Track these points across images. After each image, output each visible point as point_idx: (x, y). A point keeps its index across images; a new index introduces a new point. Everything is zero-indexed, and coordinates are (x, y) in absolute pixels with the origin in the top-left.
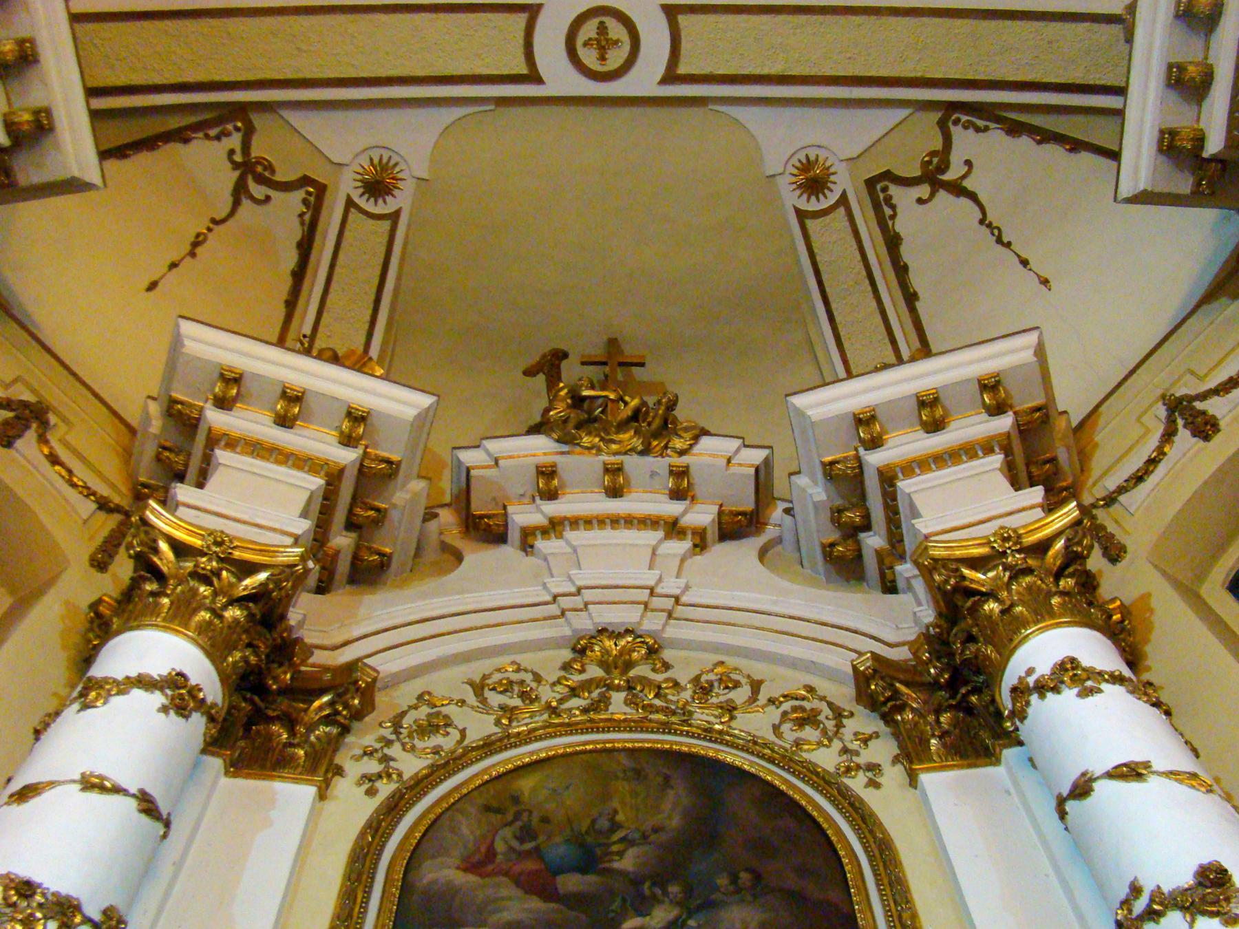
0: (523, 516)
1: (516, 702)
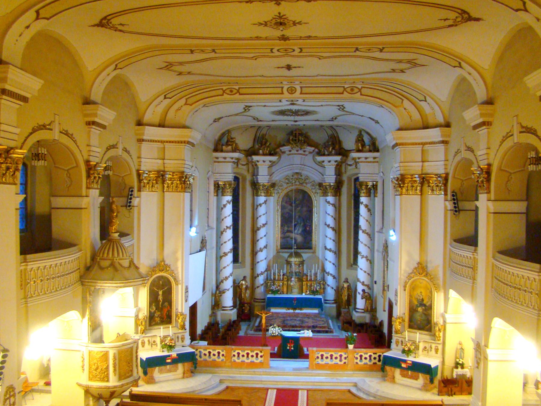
0: (287, 152)
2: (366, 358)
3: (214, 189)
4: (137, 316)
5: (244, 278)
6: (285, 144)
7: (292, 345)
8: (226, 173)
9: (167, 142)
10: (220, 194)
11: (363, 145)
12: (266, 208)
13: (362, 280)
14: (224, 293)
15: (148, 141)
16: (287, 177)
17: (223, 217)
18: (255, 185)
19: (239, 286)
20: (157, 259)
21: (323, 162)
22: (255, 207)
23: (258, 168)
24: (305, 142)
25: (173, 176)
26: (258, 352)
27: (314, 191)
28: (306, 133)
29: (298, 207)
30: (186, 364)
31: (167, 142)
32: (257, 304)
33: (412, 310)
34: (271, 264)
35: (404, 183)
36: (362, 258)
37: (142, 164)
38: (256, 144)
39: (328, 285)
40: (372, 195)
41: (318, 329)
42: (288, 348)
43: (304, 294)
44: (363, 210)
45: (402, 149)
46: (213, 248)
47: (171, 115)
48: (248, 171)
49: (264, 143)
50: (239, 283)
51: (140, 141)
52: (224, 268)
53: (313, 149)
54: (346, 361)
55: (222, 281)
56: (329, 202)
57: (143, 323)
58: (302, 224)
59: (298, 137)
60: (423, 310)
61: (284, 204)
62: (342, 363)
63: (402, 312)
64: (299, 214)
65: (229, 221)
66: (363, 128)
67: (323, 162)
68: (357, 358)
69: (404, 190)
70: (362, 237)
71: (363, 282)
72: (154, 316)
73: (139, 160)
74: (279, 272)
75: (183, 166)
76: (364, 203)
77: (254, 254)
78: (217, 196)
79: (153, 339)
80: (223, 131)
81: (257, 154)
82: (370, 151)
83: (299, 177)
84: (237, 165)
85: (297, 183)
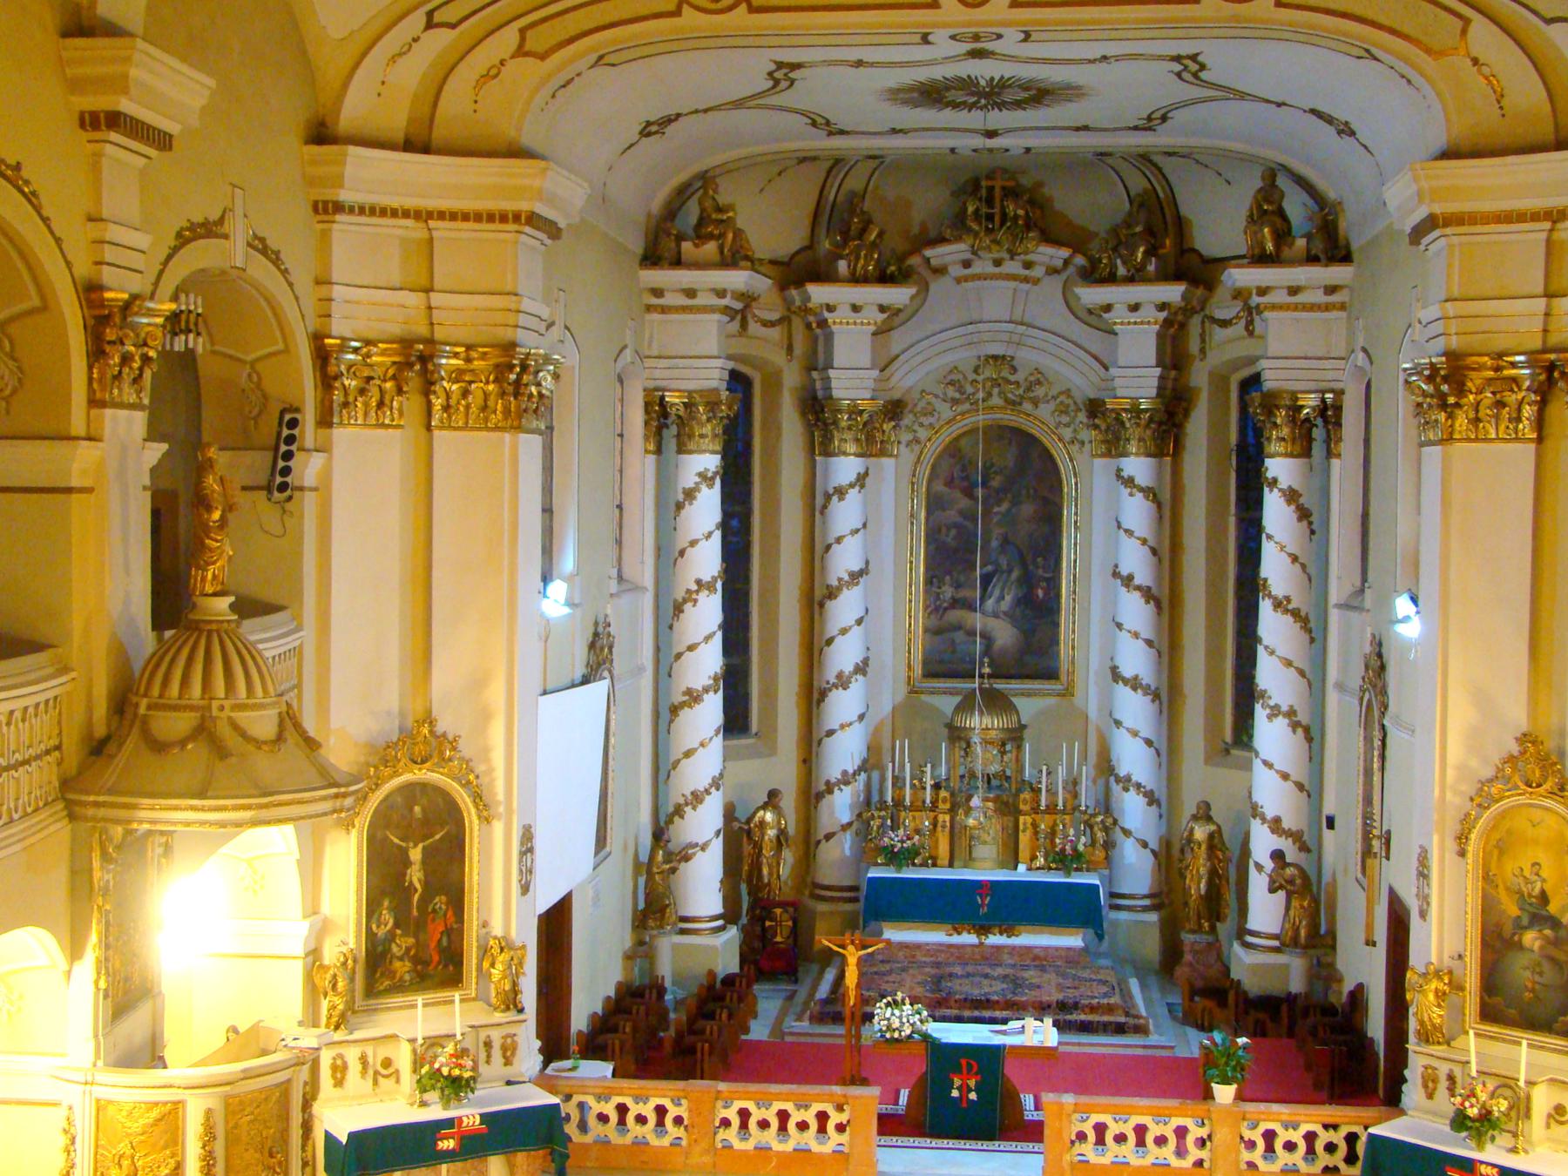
0: (955, 270)
1: (957, 395)
2: (1290, 1146)
3: (646, 423)
4: (314, 954)
5: (772, 799)
6: (948, 233)
7: (972, 1083)
8: (697, 357)
9: (441, 215)
10: (671, 444)
11: (1283, 235)
12: (865, 505)
13: (1270, 815)
14: (687, 858)
15: (362, 211)
16: (955, 377)
17: (682, 543)
18: (818, 411)
19: (749, 832)
20: (402, 714)
21: (1108, 308)
22: (817, 503)
23: (829, 337)
24: (1028, 226)
25: (468, 360)
26: (829, 1108)
27: (1067, 433)
28: (1040, 185)
29: (999, 502)
30: (520, 1157)
31: (441, 215)
32: (822, 907)
33: (1496, 943)
34: (887, 744)
35: (1461, 390)
36: (1270, 717)
37: (337, 310)
38: (822, 232)
39: (1127, 833)
40: (1318, 449)
41: (1083, 1017)
42: (955, 1093)
43: (1022, 868)
44: (1276, 513)
45: (1455, 240)
46: (641, 669)
47: (456, 104)
48: (790, 349)
49: (856, 228)
50: (749, 820)
51: (326, 211)
52: (688, 754)
53: (1065, 253)
54: (1203, 1154)
55: (678, 811)
56: (1129, 482)
57: (341, 985)
58: (1015, 574)
59: (1001, 205)
60: (1546, 938)
61: (939, 487)
62: (1188, 1163)
63: (1450, 948)
64: (1002, 531)
65: (707, 560)
66: (1282, 159)
67: (1108, 308)
68: (1251, 1145)
69: (1461, 421)
70: (1272, 626)
71: (1277, 820)
72: (387, 951)
73: (323, 291)
74: (918, 775)
75: (511, 319)
76: (1284, 483)
77: (813, 696)
78: (659, 451)
79: (384, 1051)
80: (683, 177)
81: (824, 275)
82: (1312, 259)
83: (1005, 373)
84: (744, 325)
85: (996, 400)
